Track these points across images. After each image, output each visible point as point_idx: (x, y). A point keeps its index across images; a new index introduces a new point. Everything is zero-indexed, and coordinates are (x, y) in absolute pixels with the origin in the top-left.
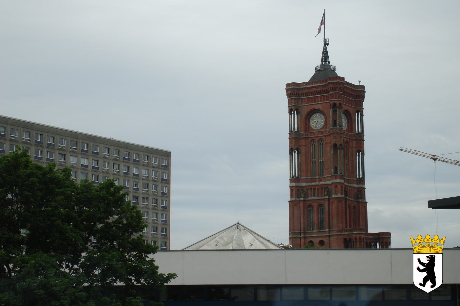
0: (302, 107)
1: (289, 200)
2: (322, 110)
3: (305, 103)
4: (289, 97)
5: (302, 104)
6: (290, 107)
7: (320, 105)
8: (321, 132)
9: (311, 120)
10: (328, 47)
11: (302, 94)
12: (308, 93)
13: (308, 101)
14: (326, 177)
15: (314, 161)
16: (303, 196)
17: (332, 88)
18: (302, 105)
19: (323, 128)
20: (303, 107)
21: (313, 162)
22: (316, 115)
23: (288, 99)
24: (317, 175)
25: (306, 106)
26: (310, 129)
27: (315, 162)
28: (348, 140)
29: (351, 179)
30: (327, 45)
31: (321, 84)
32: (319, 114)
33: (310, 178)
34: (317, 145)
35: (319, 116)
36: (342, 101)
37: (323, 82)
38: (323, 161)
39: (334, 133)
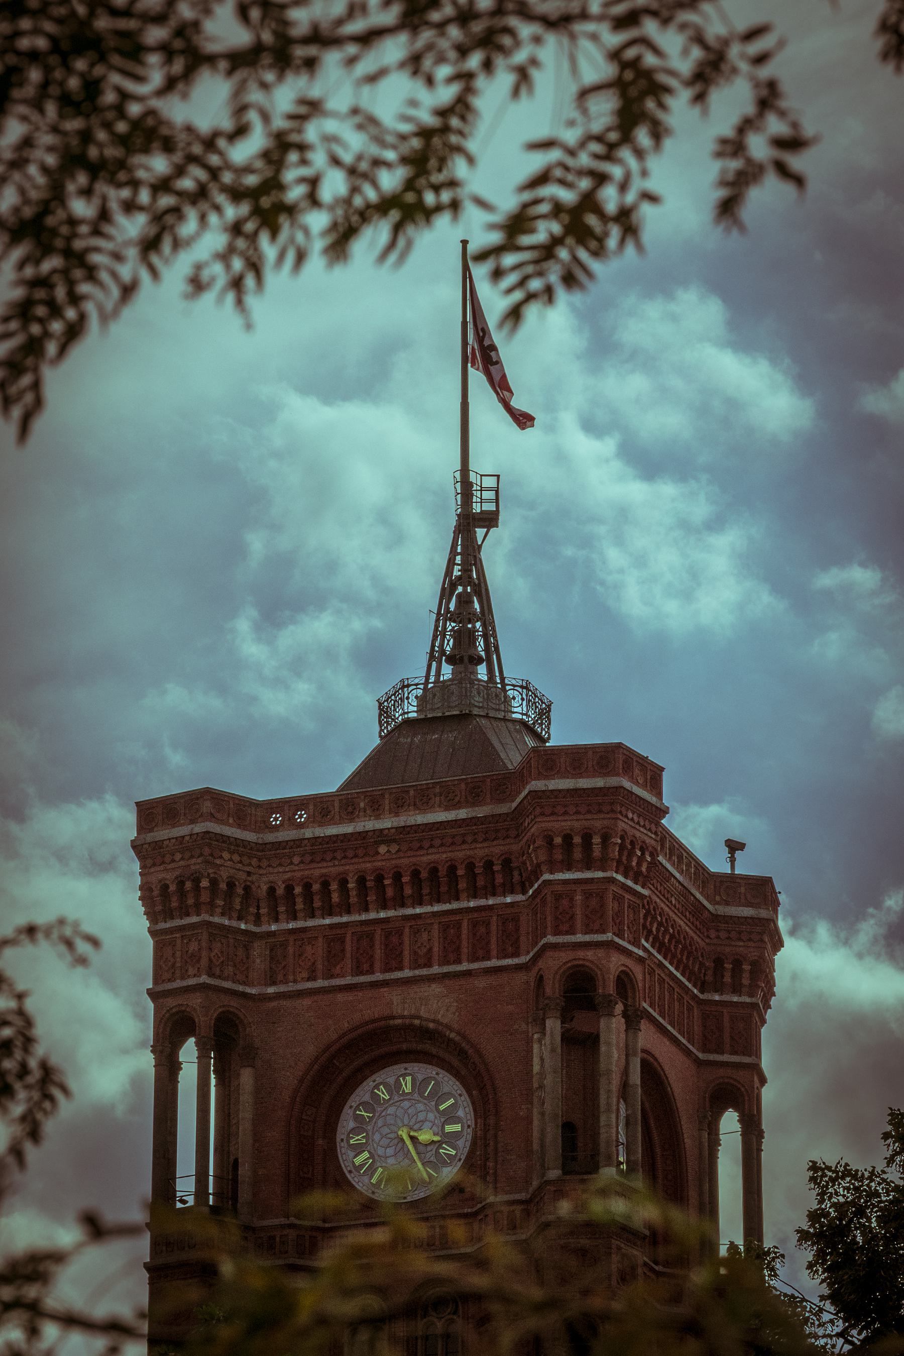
2: (458, 1033)
5: (274, 983)
6: (171, 1002)
7: (436, 988)
11: (280, 891)
12: (334, 886)
13: (333, 957)
17: (558, 840)
18: (271, 990)
22: (398, 1085)
25: (307, 1002)
30: (480, 532)
31: (462, 814)
32: (423, 1070)
35: (419, 1086)
37: (474, 795)
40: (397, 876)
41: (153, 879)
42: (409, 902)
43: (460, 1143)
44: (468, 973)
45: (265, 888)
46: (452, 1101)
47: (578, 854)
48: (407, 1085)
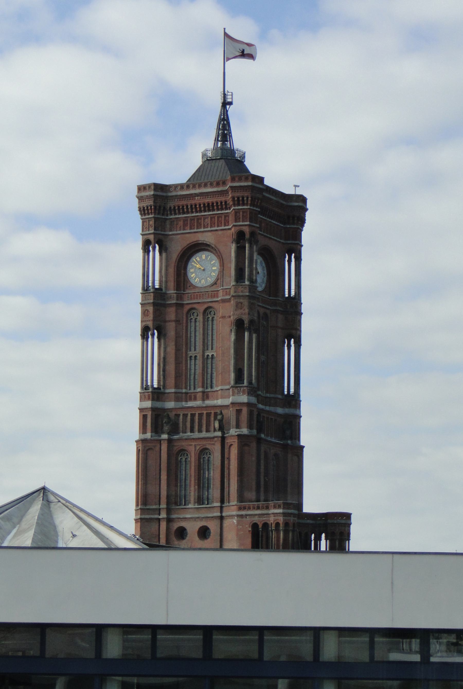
0: (171, 237)
1: (137, 438)
3: (179, 229)
4: (145, 214)
6: (146, 237)
7: (210, 234)
8: (210, 293)
9: (189, 266)
10: (231, 110)
11: (172, 208)
12: (185, 207)
14: (217, 391)
15: (193, 356)
16: (169, 431)
17: (236, 199)
18: (170, 233)
19: (215, 283)
20: (174, 236)
21: (191, 357)
23: (142, 219)
24: (200, 384)
25: (179, 236)
26: (188, 285)
27: (196, 356)
28: (268, 312)
29: (272, 396)
30: (228, 107)
31: (215, 189)
32: (207, 253)
33: (184, 391)
34: (201, 320)
35: (206, 257)
36: (257, 227)
37: (218, 184)
38: (213, 355)
39: (239, 296)
40: (200, 205)
41: (142, 205)
42: (203, 212)
43: (216, 272)
44: (216, 230)
45: (169, 207)
46: (214, 261)
47: (241, 202)
48: (204, 257)
